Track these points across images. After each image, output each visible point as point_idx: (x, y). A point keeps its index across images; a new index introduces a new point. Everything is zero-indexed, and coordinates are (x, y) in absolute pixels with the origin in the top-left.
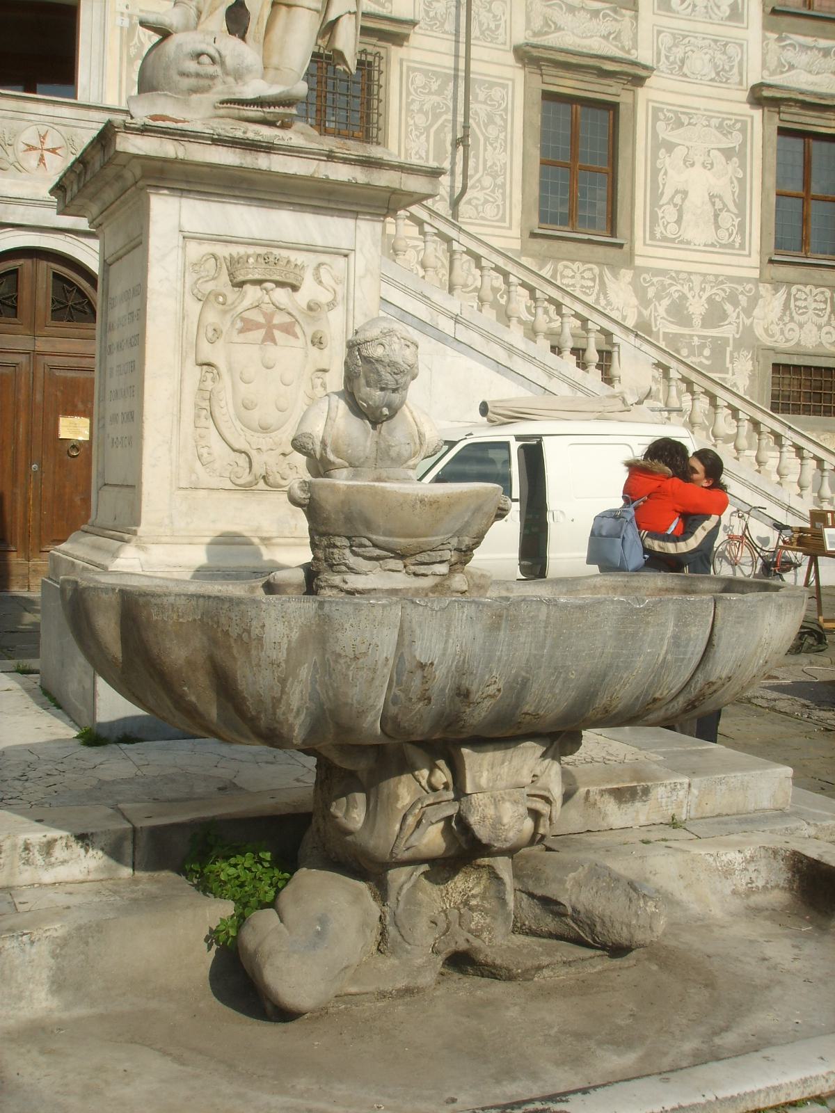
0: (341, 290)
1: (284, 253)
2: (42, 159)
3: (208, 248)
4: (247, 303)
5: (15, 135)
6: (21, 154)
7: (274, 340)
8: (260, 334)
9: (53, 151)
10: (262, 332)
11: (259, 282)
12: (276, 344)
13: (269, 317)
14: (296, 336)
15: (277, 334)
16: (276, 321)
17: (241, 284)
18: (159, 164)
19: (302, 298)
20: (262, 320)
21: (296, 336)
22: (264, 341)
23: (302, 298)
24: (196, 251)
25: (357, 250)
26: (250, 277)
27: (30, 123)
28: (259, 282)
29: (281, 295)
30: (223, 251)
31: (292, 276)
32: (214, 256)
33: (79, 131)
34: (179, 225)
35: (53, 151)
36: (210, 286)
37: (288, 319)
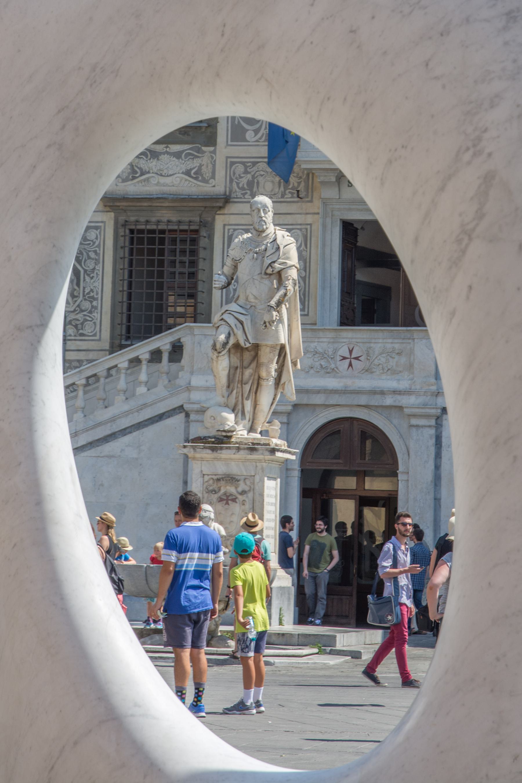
0: (252, 486)
2: (350, 365)
3: (210, 476)
5: (335, 351)
6: (338, 363)
7: (228, 504)
8: (225, 502)
9: (357, 358)
10: (225, 502)
14: (236, 502)
15: (230, 502)
16: (230, 498)
20: (225, 498)
21: (236, 502)
23: (240, 490)
27: (344, 344)
32: (213, 479)
33: (372, 345)
35: (357, 358)
36: (211, 488)
37: (234, 497)
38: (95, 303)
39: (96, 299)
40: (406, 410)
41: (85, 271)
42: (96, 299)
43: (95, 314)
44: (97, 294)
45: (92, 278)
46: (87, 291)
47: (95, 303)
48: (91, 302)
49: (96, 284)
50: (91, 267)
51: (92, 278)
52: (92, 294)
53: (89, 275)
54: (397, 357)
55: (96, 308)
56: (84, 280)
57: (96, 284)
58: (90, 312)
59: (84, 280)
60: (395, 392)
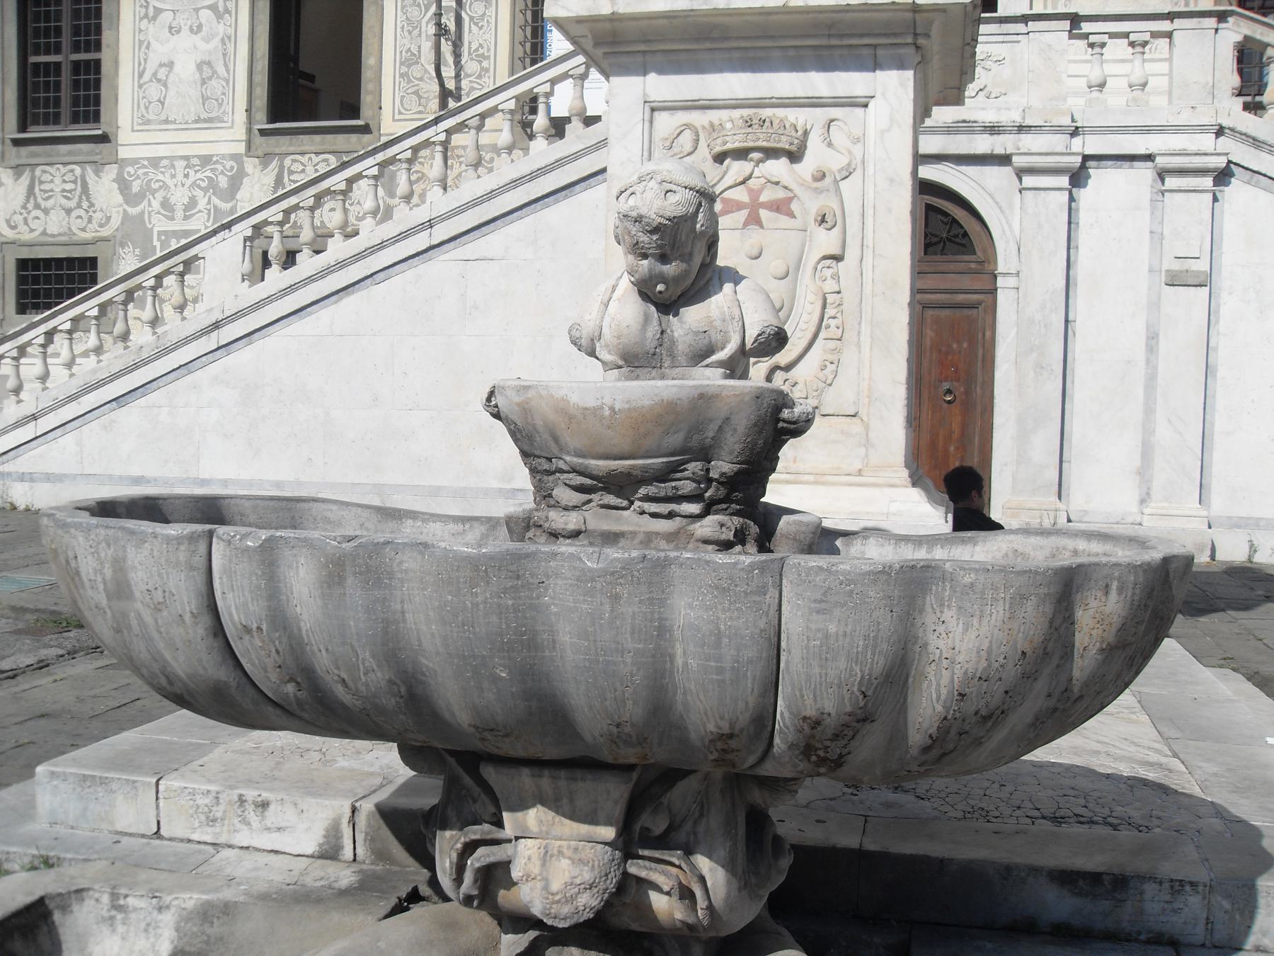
1: (780, 112)
4: (728, 181)
7: (759, 223)
10: (743, 214)
11: (741, 154)
12: (762, 227)
13: (755, 194)
15: (764, 213)
16: (763, 198)
17: (720, 158)
18: (608, 26)
19: (807, 167)
22: (746, 224)
24: (666, 123)
25: (878, 95)
26: (729, 146)
28: (741, 154)
29: (777, 168)
30: (699, 119)
31: (784, 138)
32: (688, 126)
34: (645, 94)
37: (780, 194)
38: (485, 64)
39: (488, 58)
40: (1015, 159)
41: (471, 18)
42: (488, 58)
43: (486, 80)
44: (489, 50)
45: (481, 28)
46: (474, 47)
47: (485, 64)
48: (480, 62)
49: (487, 36)
50: (480, 13)
51: (481, 28)
52: (481, 51)
53: (476, 24)
54: (994, 66)
55: (487, 70)
56: (470, 31)
57: (487, 36)
58: (479, 77)
59: (470, 31)
60: (993, 130)
